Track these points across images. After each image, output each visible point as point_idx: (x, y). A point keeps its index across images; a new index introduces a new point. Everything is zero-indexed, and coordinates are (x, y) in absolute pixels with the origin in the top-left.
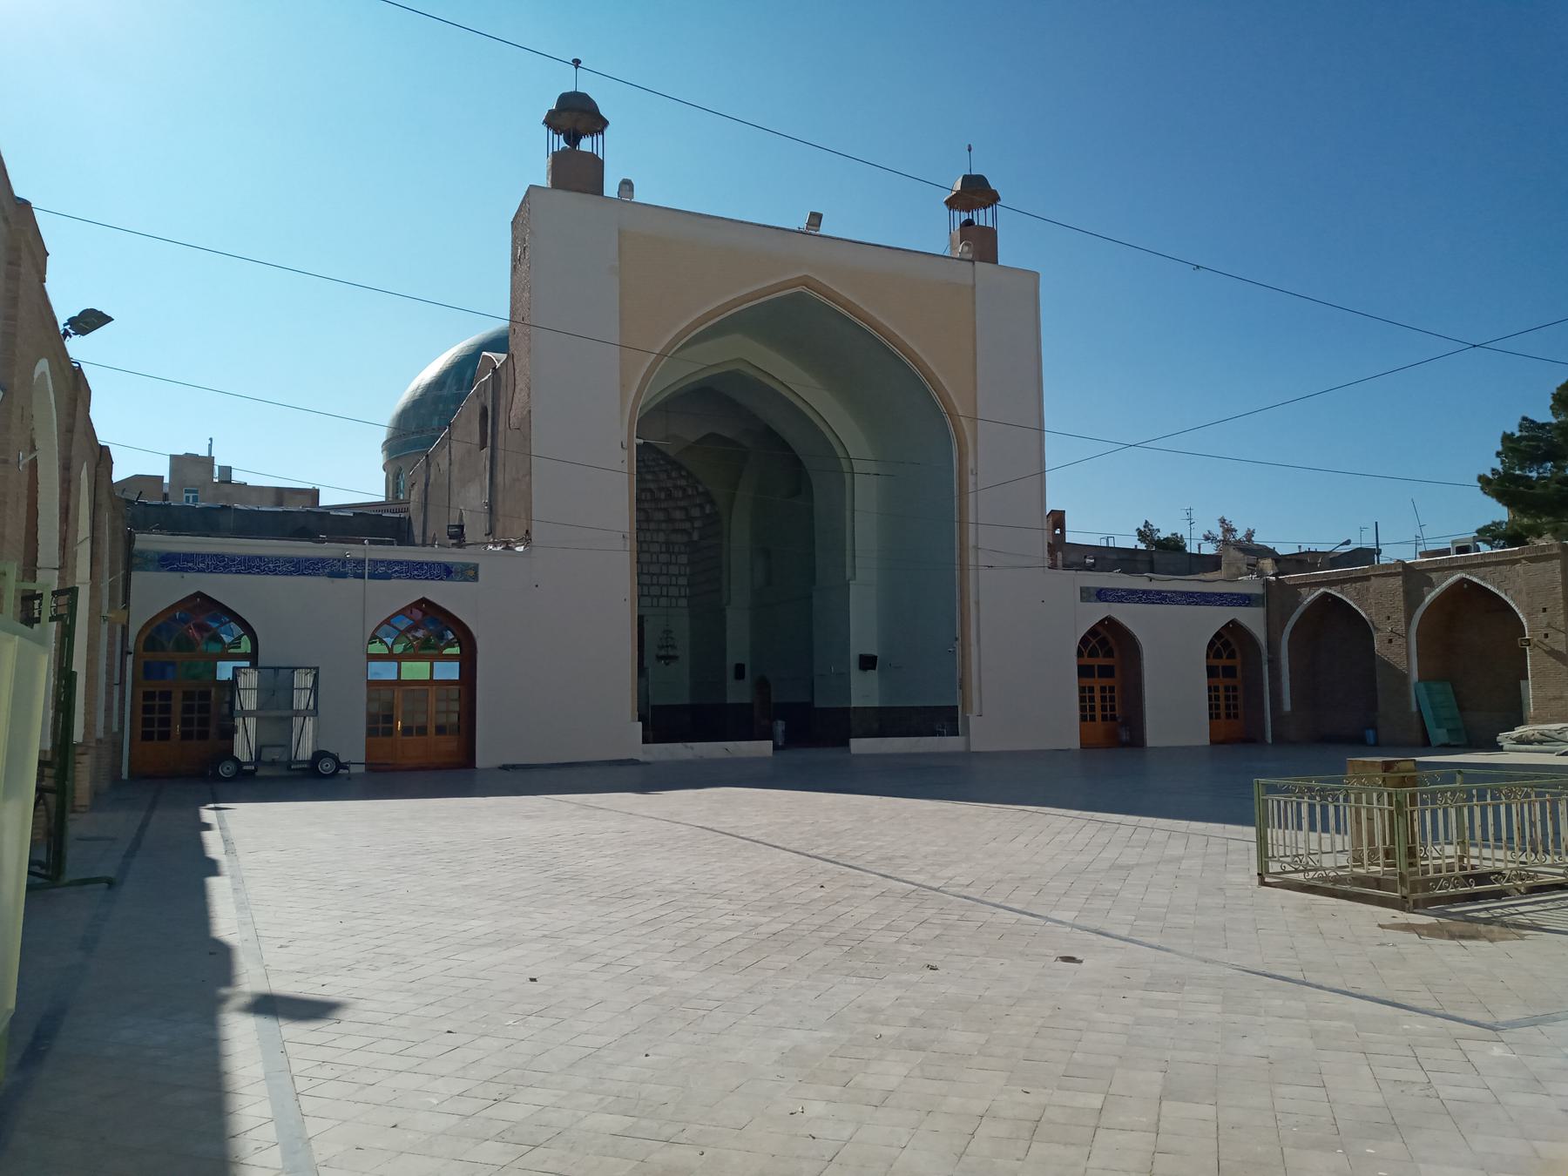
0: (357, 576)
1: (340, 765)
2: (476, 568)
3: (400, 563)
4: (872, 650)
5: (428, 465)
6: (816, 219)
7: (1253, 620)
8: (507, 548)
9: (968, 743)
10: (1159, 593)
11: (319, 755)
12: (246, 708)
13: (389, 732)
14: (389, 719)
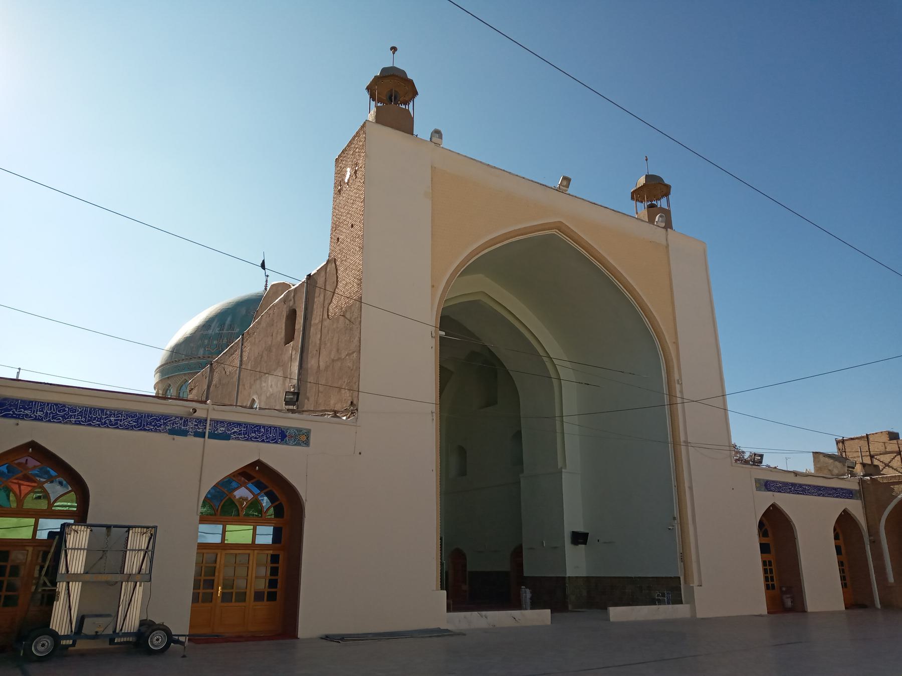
0: (197, 435)
1: (171, 639)
2: (308, 433)
3: (239, 424)
4: (581, 529)
5: (212, 370)
6: (567, 180)
7: (855, 508)
8: (335, 416)
9: (693, 610)
10: (801, 485)
11: (147, 627)
12: (72, 570)
13: (209, 598)
14: (210, 584)
